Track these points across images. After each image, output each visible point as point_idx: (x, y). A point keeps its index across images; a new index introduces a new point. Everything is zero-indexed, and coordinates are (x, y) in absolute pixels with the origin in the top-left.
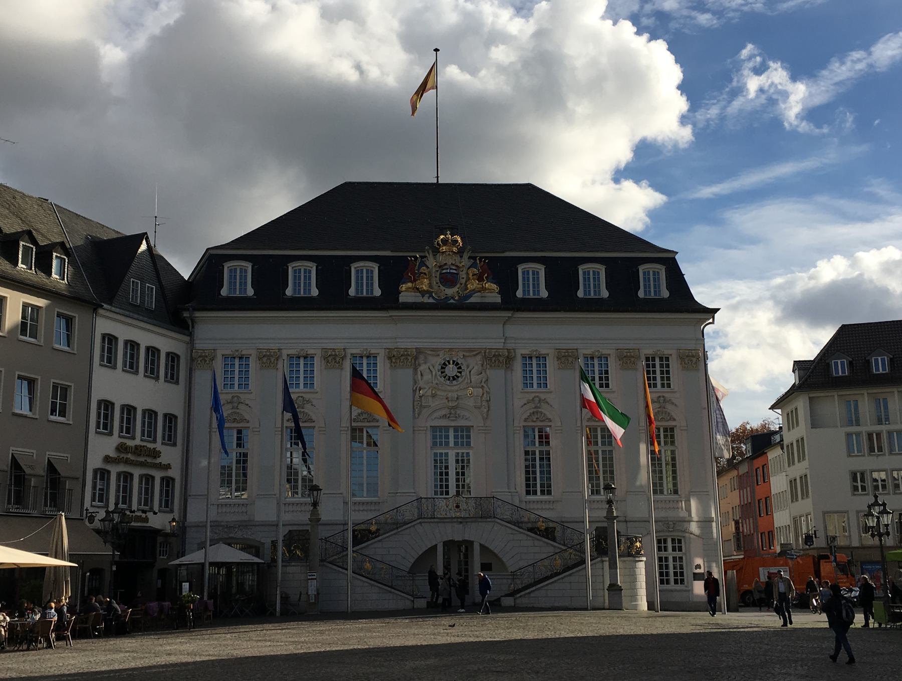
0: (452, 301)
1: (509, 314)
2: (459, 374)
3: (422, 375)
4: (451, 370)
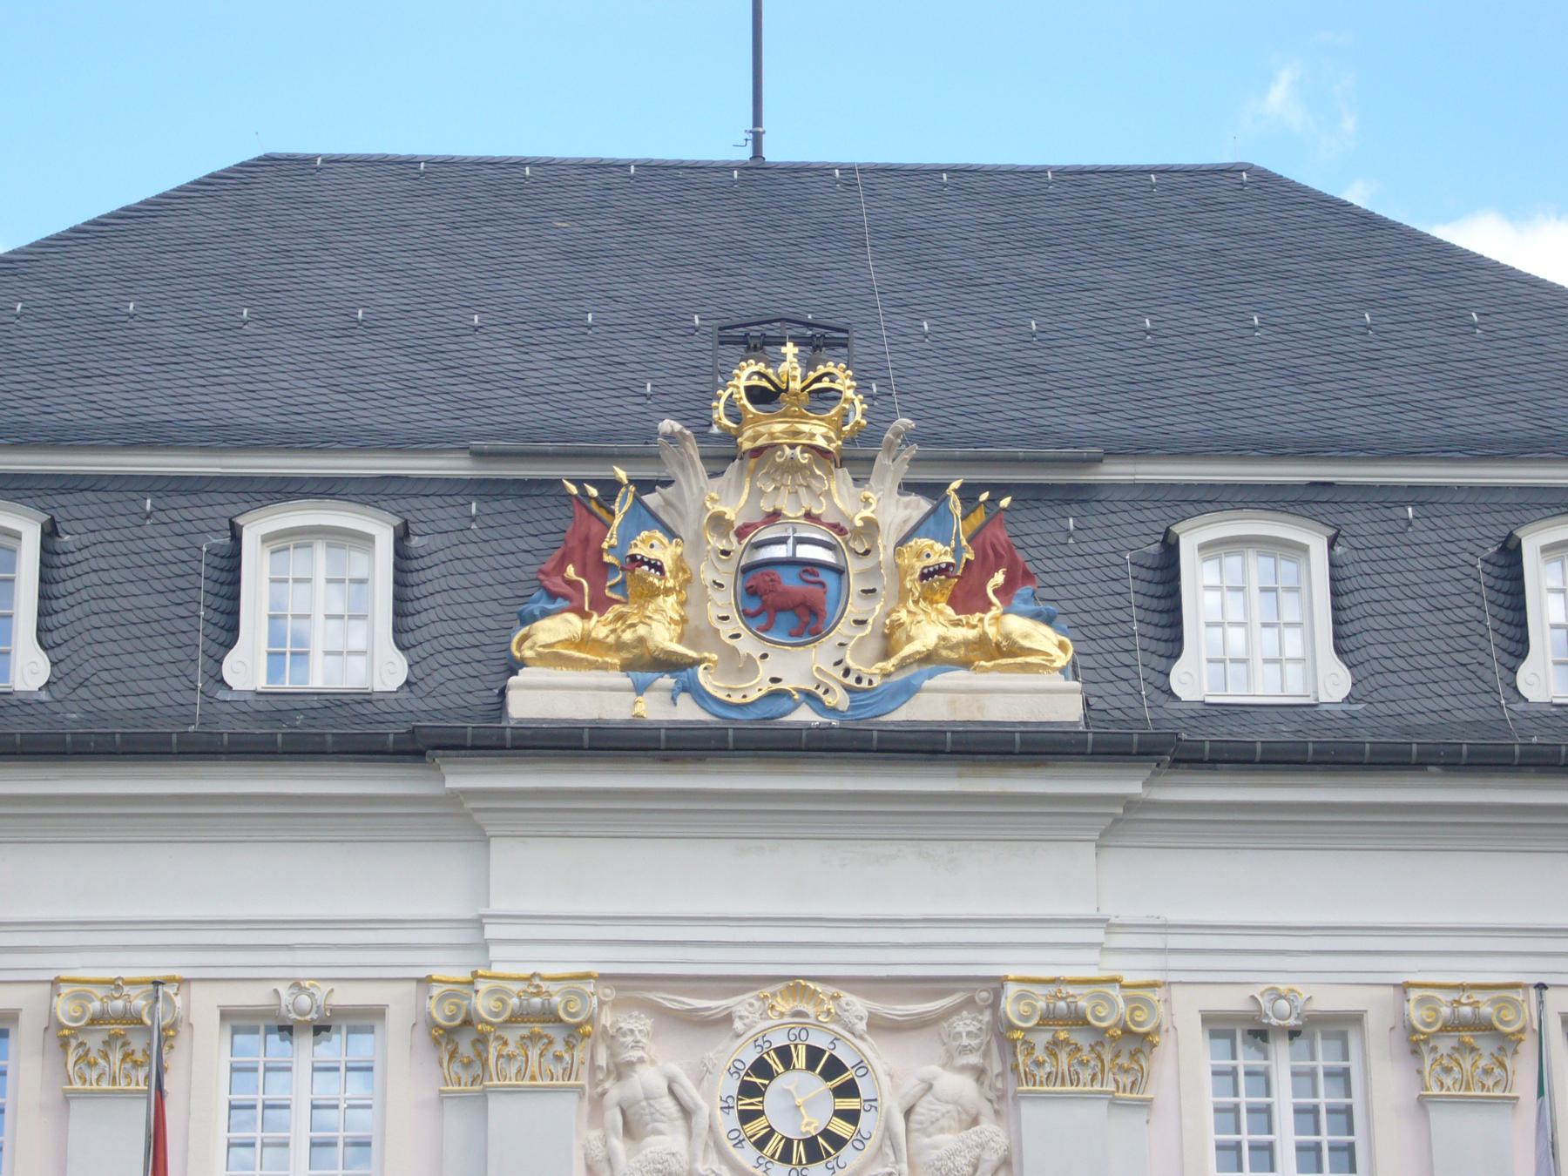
0: (805, 715)
1: (1128, 784)
2: (842, 1128)
3: (631, 1129)
4: (799, 1103)
